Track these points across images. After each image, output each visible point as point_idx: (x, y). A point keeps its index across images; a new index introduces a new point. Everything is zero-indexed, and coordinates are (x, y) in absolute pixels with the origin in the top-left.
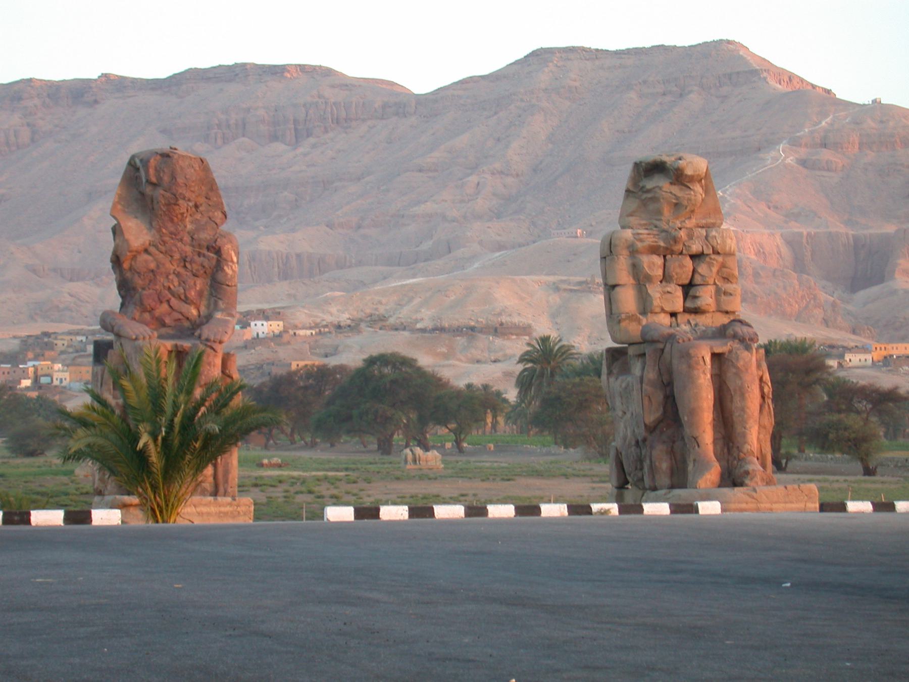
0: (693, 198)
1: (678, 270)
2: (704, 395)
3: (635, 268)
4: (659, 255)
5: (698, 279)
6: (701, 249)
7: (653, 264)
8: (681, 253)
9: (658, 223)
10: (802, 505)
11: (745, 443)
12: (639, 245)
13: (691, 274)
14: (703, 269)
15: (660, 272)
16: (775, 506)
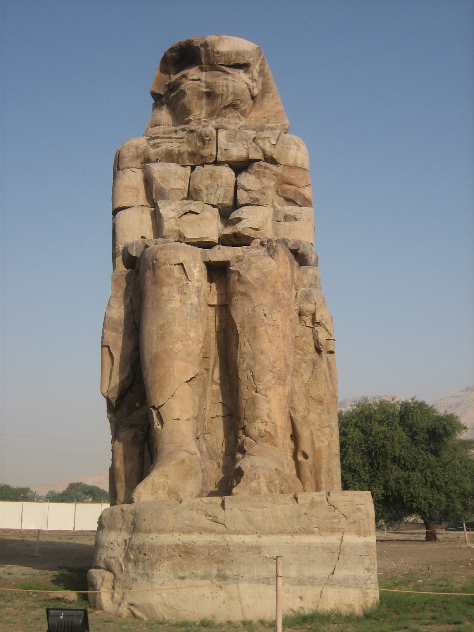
0: (231, 84)
1: (209, 182)
2: (178, 330)
3: (148, 181)
4: (185, 166)
5: (243, 196)
6: (243, 154)
7: (172, 176)
8: (216, 163)
9: (186, 127)
10: (333, 539)
11: (257, 418)
12: (152, 151)
13: (233, 189)
14: (247, 180)
15: (182, 185)
16: (265, 540)
